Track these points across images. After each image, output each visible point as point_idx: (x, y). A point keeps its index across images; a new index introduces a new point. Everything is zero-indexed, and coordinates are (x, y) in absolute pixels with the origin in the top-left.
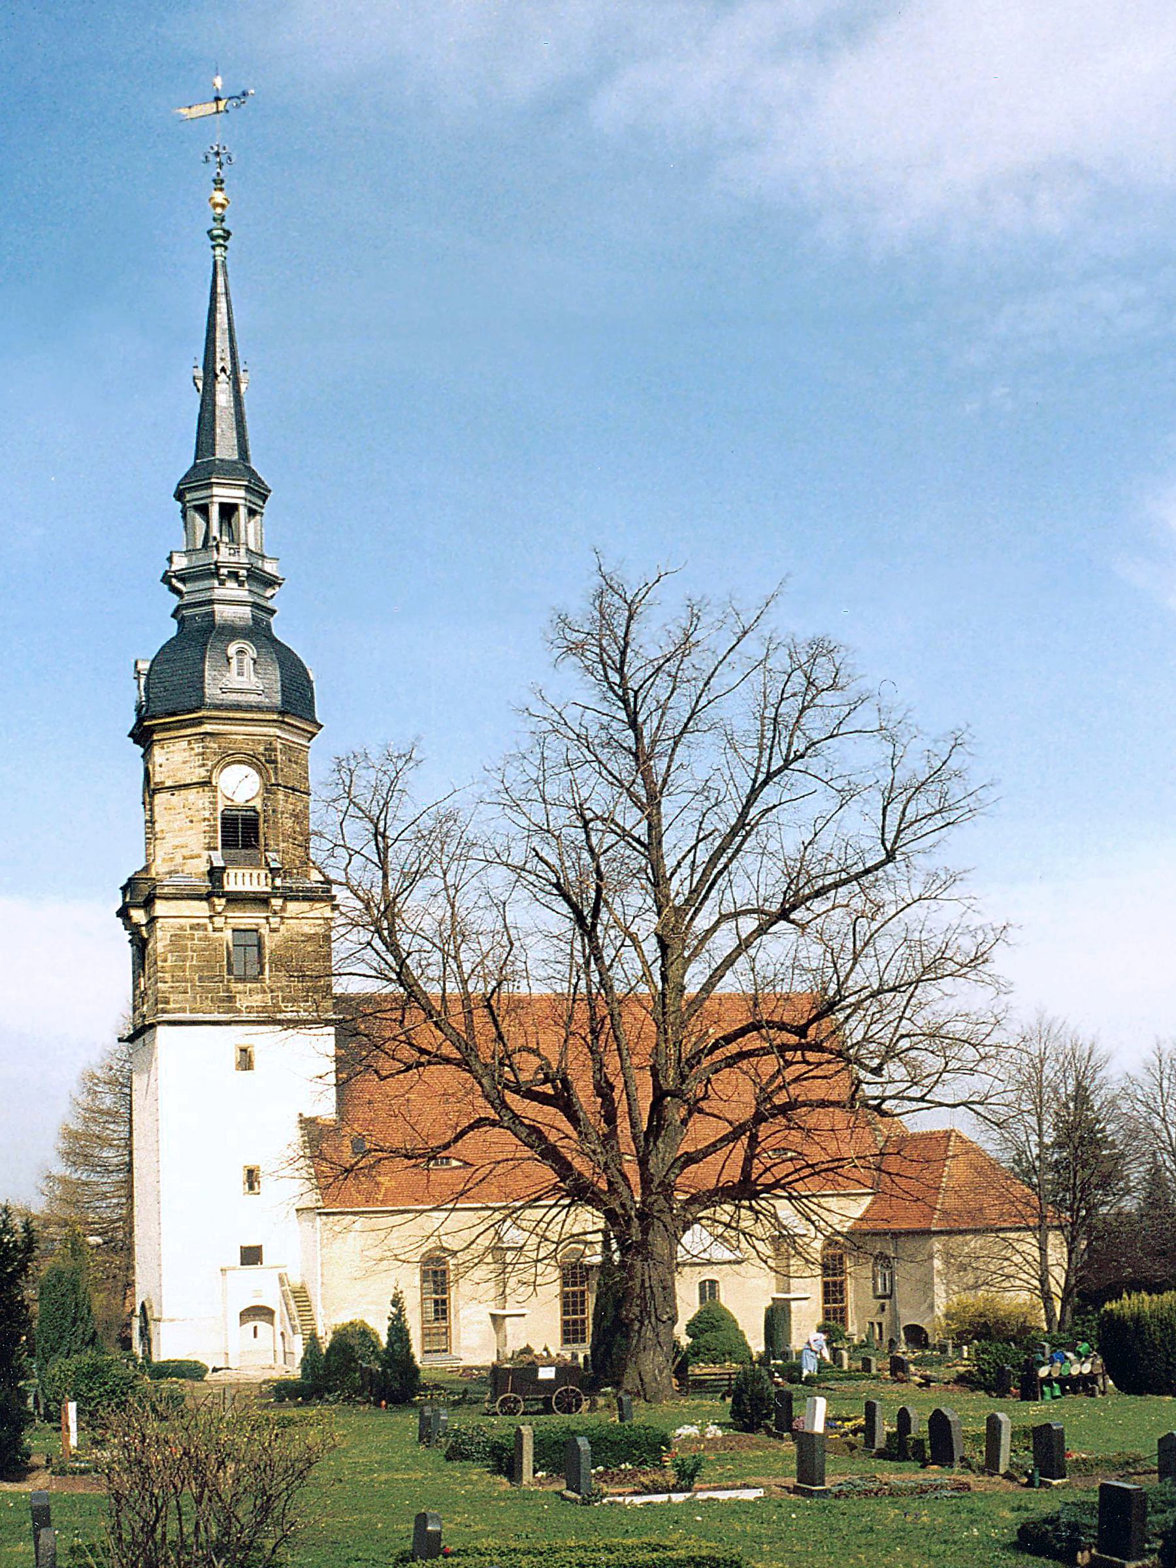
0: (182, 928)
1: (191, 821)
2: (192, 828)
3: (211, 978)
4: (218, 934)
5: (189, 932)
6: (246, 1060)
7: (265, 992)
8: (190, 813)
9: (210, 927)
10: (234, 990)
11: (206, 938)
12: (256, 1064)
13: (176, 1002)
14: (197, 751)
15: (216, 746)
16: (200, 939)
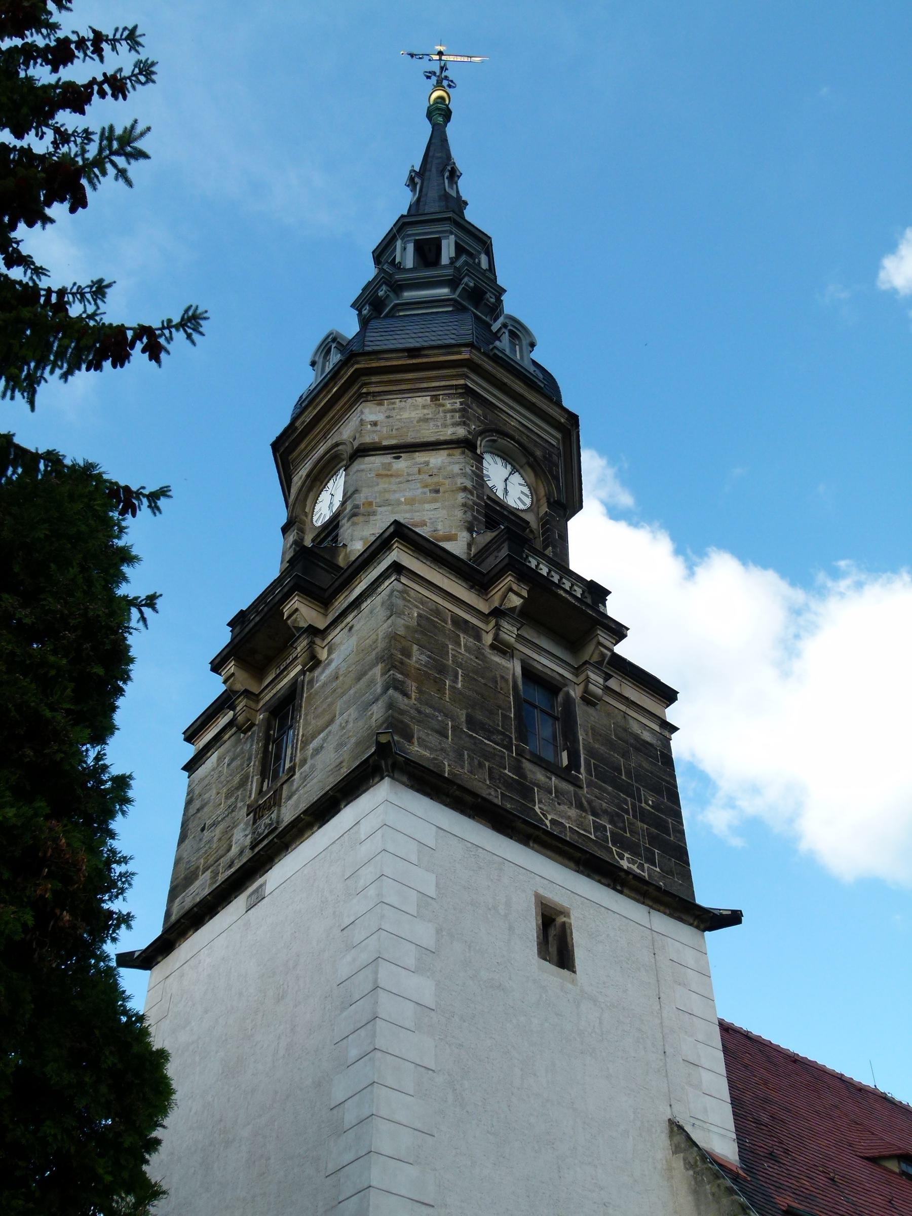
0: (437, 612)
1: (437, 491)
2: (435, 501)
3: (489, 732)
4: (497, 659)
5: (449, 626)
6: (555, 940)
7: (580, 806)
8: (435, 479)
9: (488, 639)
10: (530, 776)
11: (479, 655)
12: (580, 956)
13: (422, 743)
14: (449, 406)
15: (480, 412)
16: (468, 649)
